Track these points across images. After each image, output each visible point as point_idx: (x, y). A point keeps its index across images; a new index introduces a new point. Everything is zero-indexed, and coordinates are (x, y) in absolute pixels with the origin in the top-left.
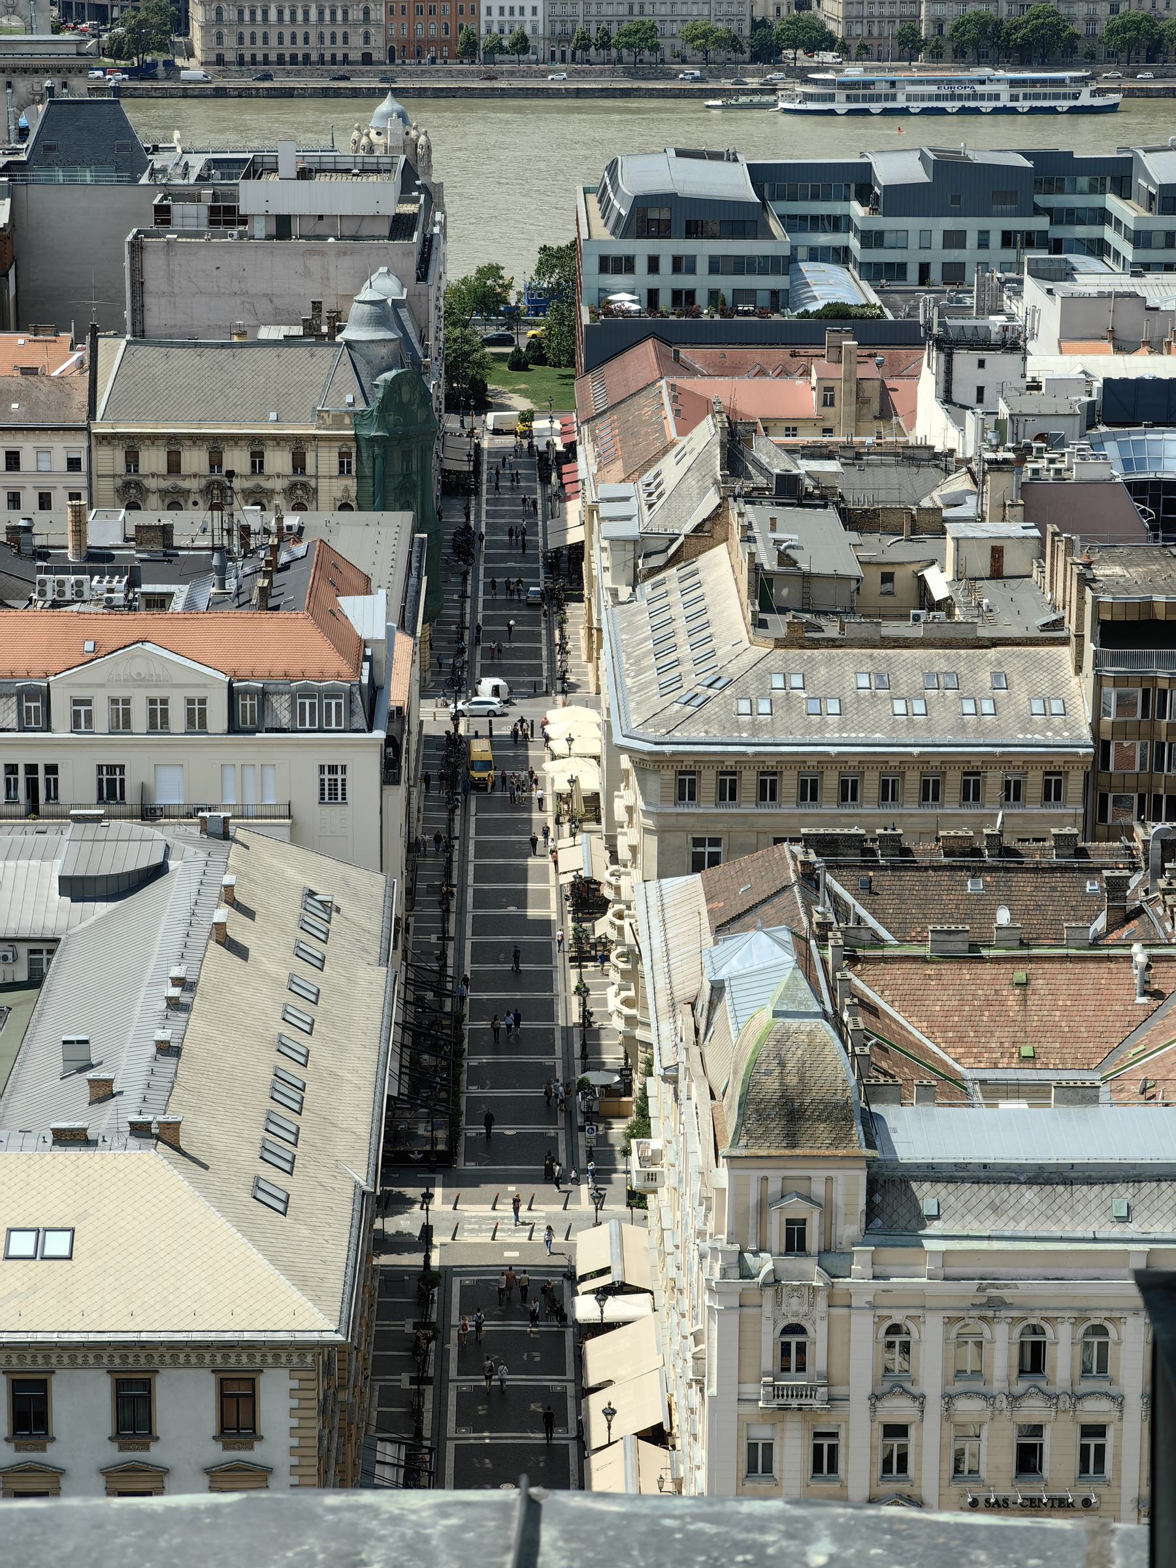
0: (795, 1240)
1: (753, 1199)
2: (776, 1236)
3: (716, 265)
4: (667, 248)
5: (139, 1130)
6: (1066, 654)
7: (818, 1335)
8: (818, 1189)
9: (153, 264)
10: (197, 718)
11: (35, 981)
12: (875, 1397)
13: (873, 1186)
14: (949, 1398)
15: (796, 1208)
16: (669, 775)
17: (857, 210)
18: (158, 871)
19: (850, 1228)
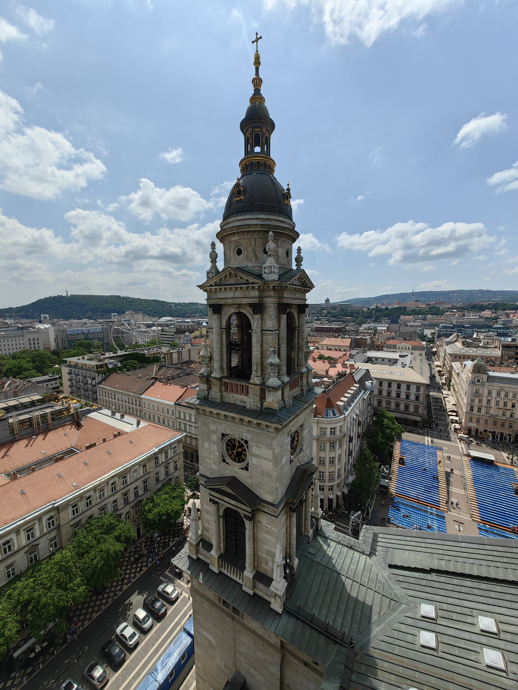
0: (478, 381)
1: (474, 377)
2: (476, 381)
3: (449, 331)
4: (445, 330)
5: (409, 367)
6: (498, 349)
7: (481, 390)
8: (481, 377)
9: (400, 328)
10: (409, 349)
11: (396, 363)
12: (487, 397)
13: (488, 377)
14: (496, 398)
15: (479, 378)
16: (454, 356)
17: (463, 329)
18: (407, 355)
19: (485, 381)
